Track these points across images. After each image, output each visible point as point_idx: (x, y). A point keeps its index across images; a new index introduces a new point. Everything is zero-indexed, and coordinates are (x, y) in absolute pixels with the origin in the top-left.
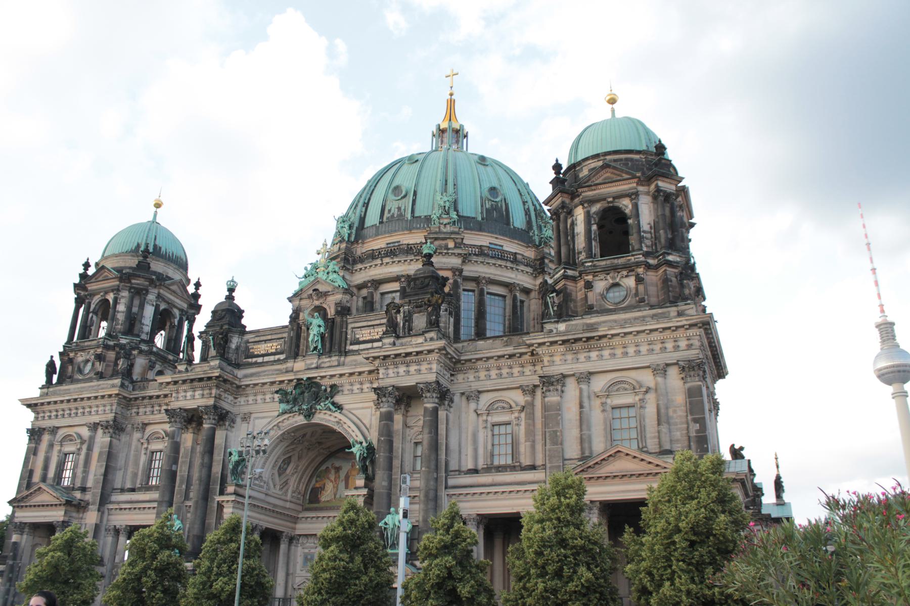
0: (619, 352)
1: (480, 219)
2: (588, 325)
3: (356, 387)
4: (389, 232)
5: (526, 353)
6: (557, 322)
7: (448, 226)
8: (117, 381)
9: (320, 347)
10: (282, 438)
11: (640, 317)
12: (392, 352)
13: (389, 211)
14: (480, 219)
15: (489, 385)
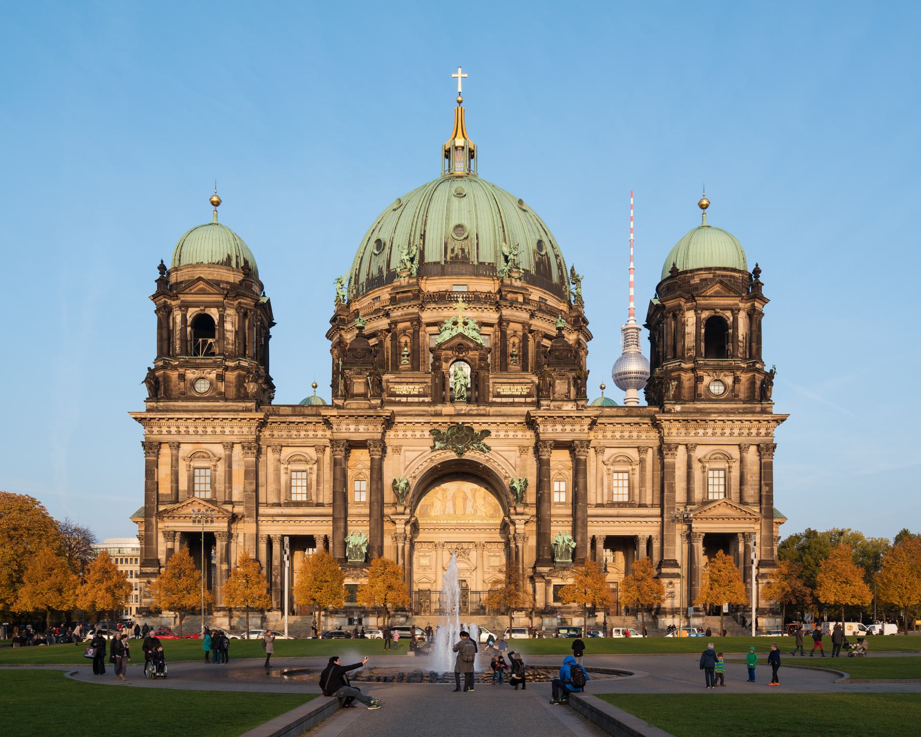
0: (719, 431)
1: (533, 272)
2: (697, 409)
3: (502, 434)
4: (456, 275)
5: (647, 424)
6: (675, 404)
7: (518, 280)
8: (251, 405)
9: (465, 396)
10: (432, 468)
11: (735, 408)
12: (555, 414)
13: (453, 250)
14: (533, 272)
15: (614, 443)
